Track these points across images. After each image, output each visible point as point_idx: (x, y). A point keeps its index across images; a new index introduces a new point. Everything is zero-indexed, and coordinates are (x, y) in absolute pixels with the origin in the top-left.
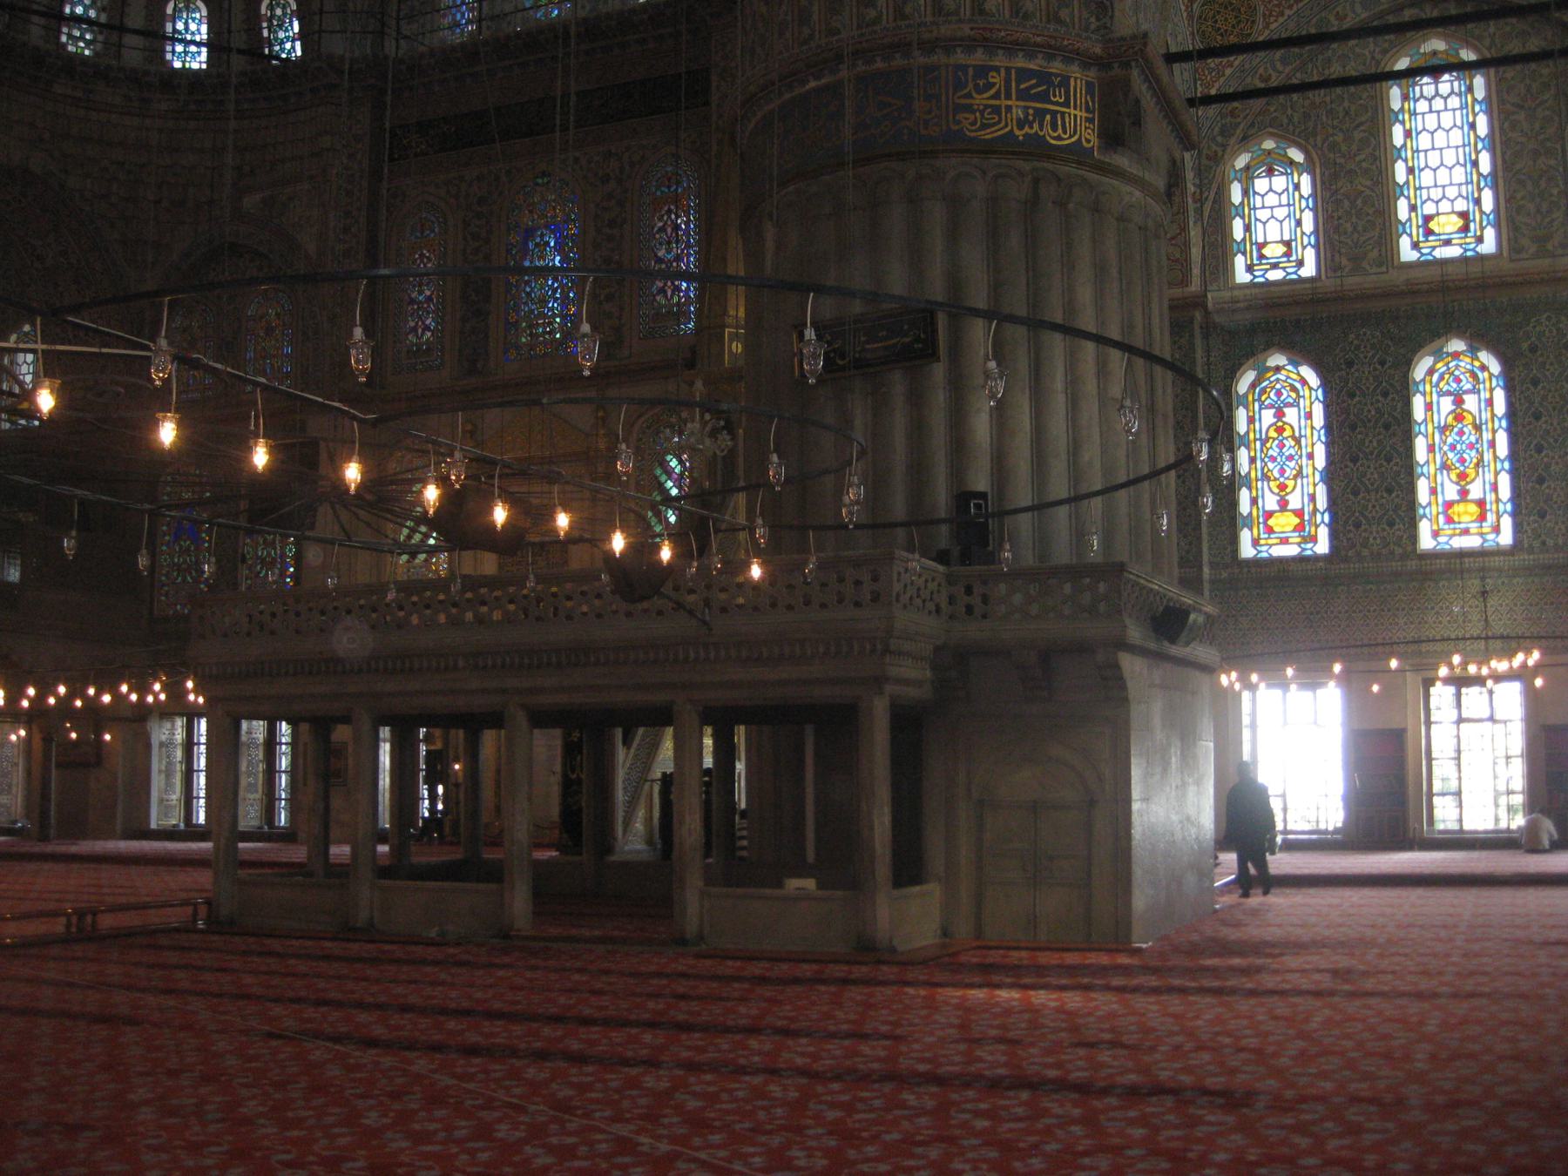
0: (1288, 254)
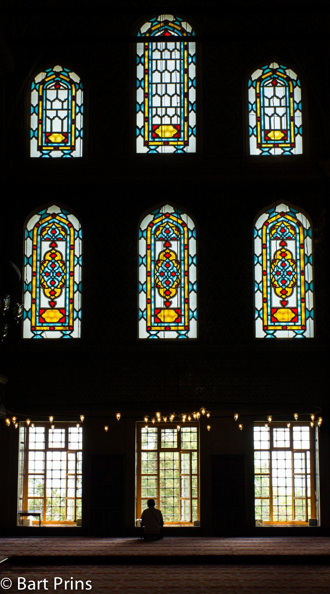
0: (65, 142)
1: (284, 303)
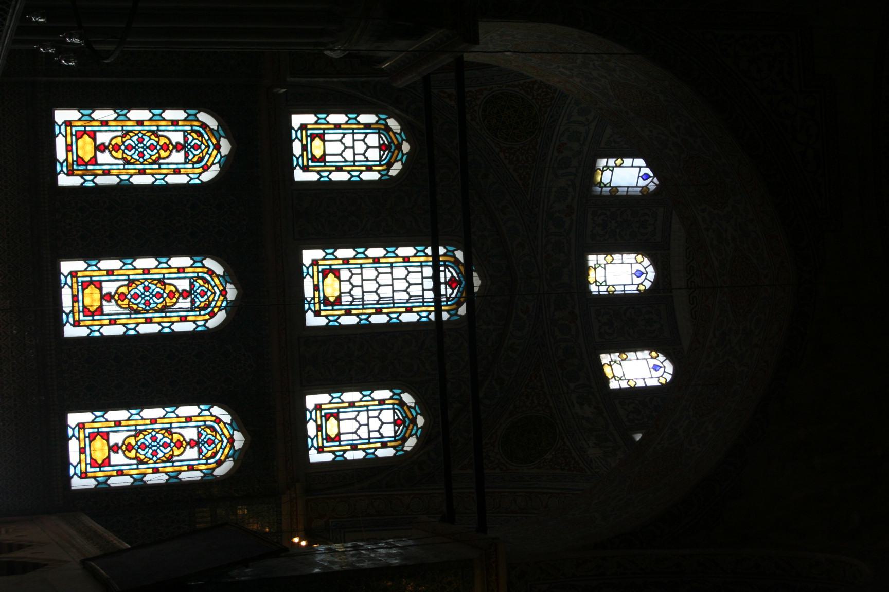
0: (314, 158)
1: (115, 448)
